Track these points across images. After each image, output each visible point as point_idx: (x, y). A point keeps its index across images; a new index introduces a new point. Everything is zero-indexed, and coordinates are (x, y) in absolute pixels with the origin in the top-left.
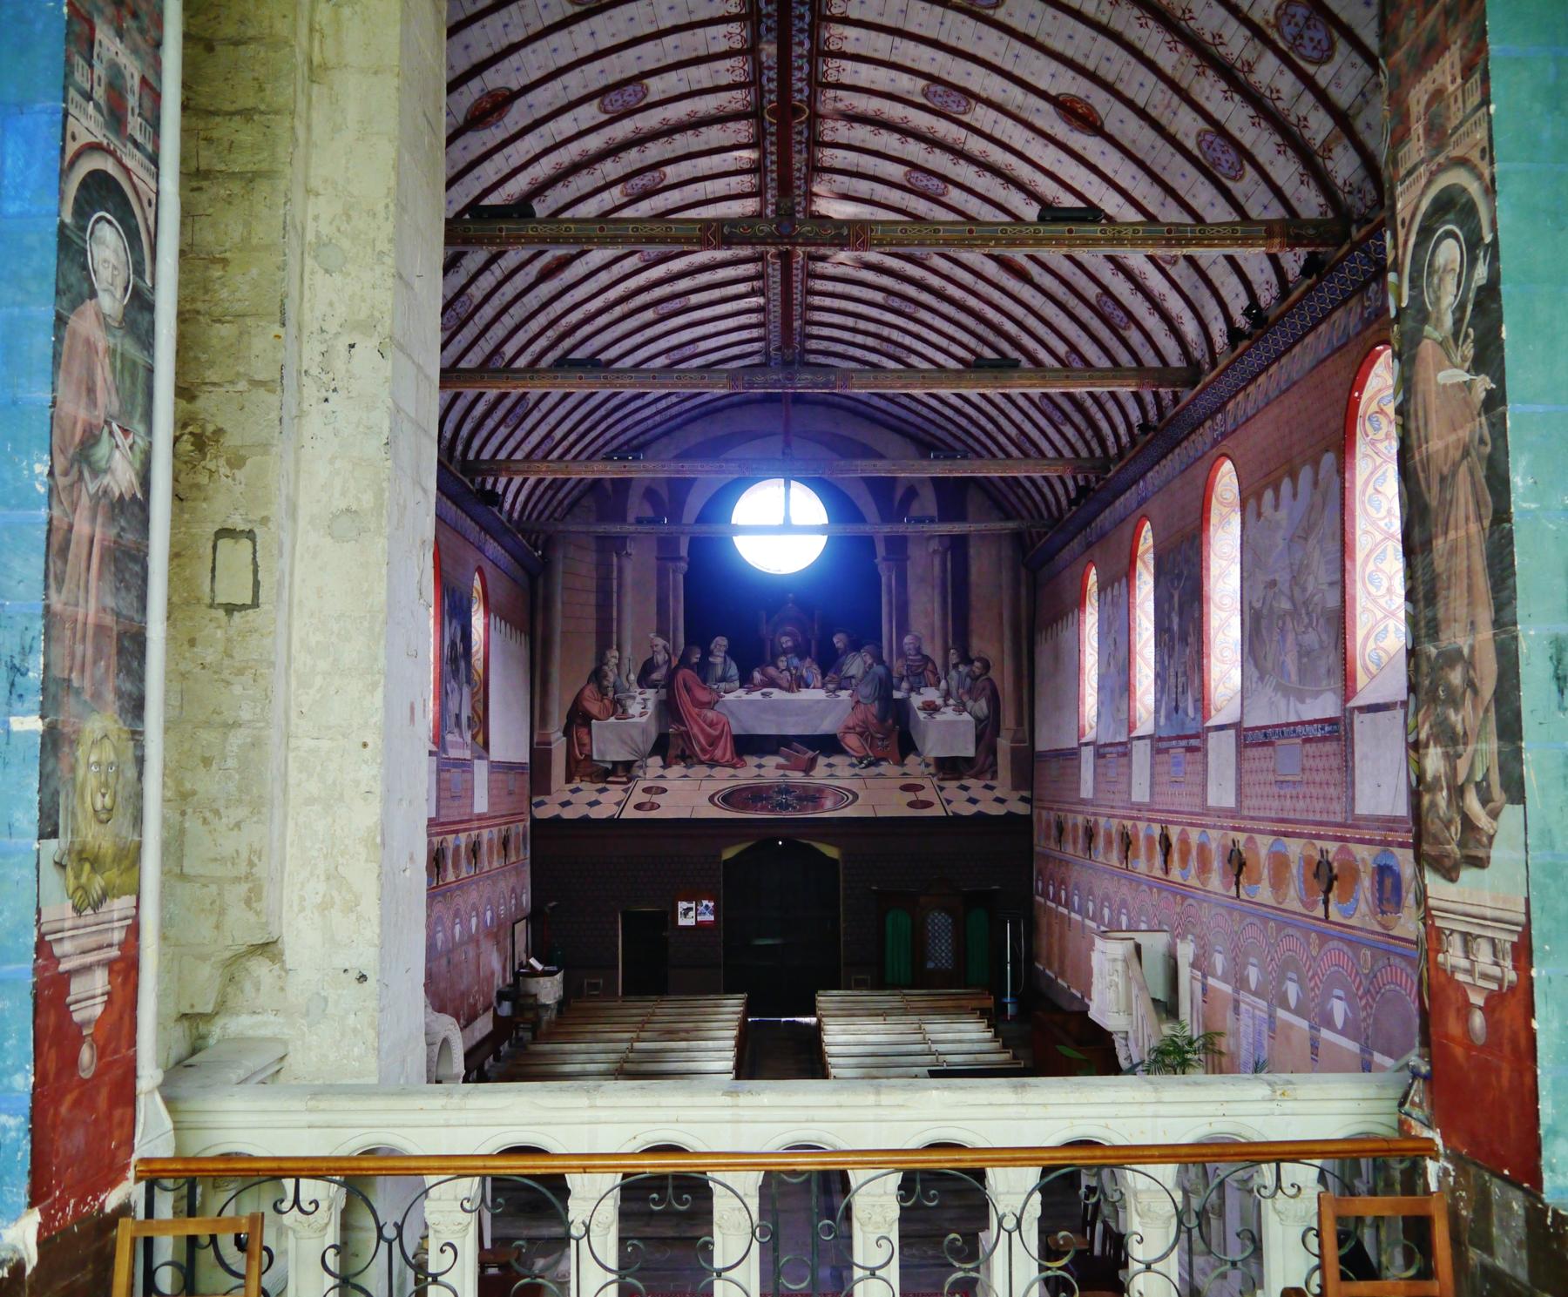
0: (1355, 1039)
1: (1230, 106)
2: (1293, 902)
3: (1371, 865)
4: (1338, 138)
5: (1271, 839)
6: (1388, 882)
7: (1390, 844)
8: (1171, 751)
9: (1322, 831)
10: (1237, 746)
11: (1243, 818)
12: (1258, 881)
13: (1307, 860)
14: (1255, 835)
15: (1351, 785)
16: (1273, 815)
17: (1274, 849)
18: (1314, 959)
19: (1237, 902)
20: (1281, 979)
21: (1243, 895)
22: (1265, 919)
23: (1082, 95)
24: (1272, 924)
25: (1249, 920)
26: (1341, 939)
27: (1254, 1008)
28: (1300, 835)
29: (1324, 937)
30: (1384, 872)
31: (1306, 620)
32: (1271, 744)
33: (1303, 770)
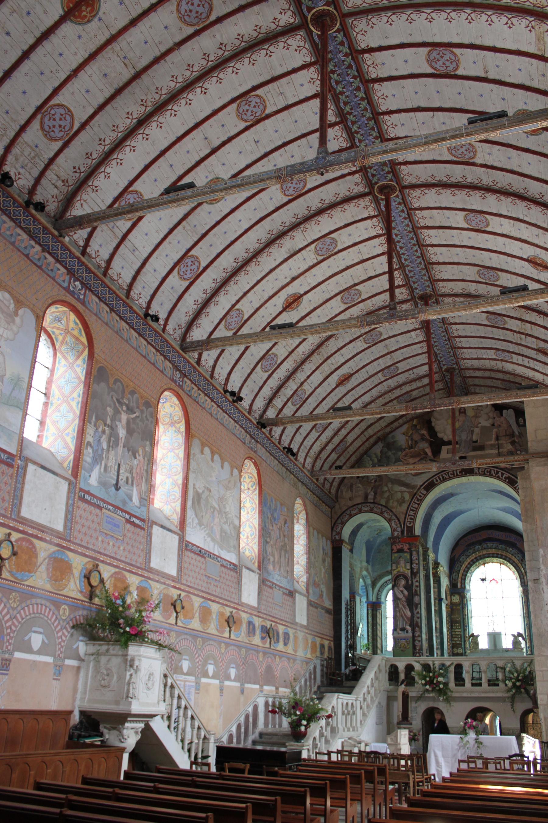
0: (239, 681)
1: (285, 370)
2: (212, 629)
3: (246, 620)
4: (276, 410)
5: (202, 600)
6: (251, 627)
7: (252, 614)
8: (104, 510)
9: (229, 604)
10: (179, 546)
11: (181, 584)
12: (192, 618)
13: (221, 614)
14: (191, 596)
15: (240, 590)
16: (203, 589)
17: (203, 605)
18: (223, 654)
19: (175, 627)
20: (205, 663)
21: (179, 623)
22: (195, 637)
23: (299, 308)
24: (199, 639)
25: (183, 637)
26: (235, 645)
27: (185, 681)
28: (218, 603)
29: (227, 645)
30: (250, 623)
31: (225, 520)
32: (205, 558)
33: (220, 576)
